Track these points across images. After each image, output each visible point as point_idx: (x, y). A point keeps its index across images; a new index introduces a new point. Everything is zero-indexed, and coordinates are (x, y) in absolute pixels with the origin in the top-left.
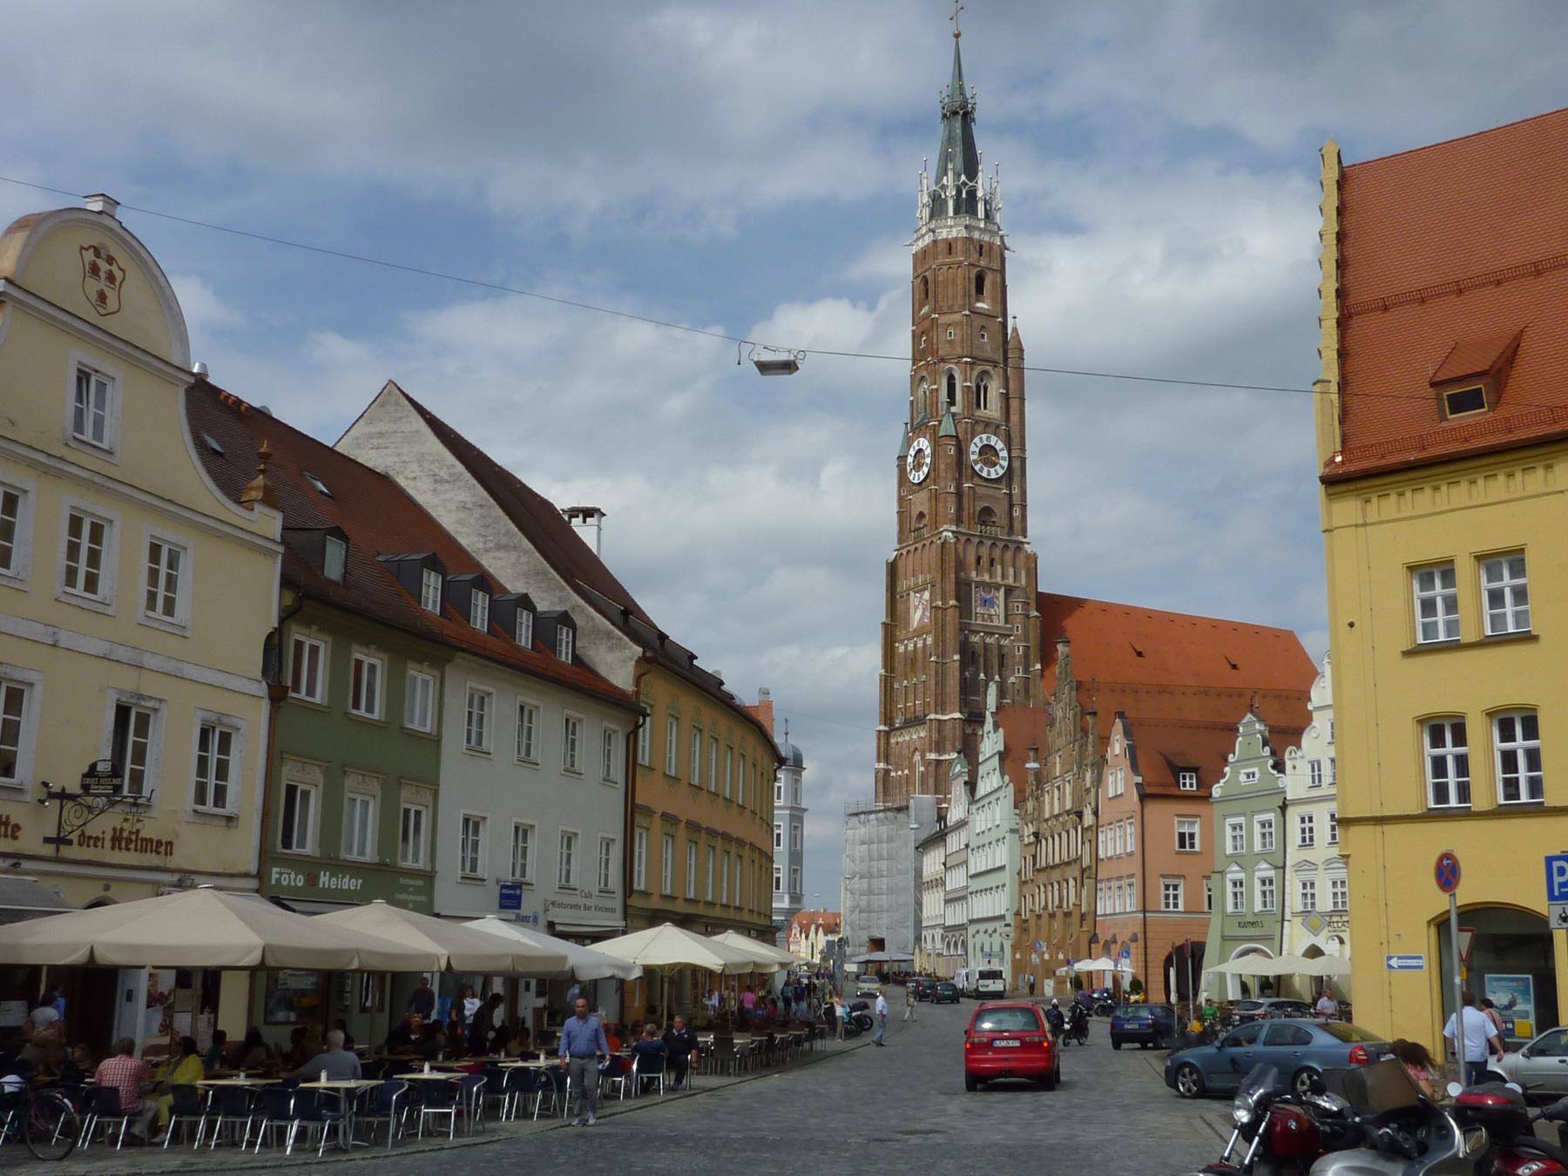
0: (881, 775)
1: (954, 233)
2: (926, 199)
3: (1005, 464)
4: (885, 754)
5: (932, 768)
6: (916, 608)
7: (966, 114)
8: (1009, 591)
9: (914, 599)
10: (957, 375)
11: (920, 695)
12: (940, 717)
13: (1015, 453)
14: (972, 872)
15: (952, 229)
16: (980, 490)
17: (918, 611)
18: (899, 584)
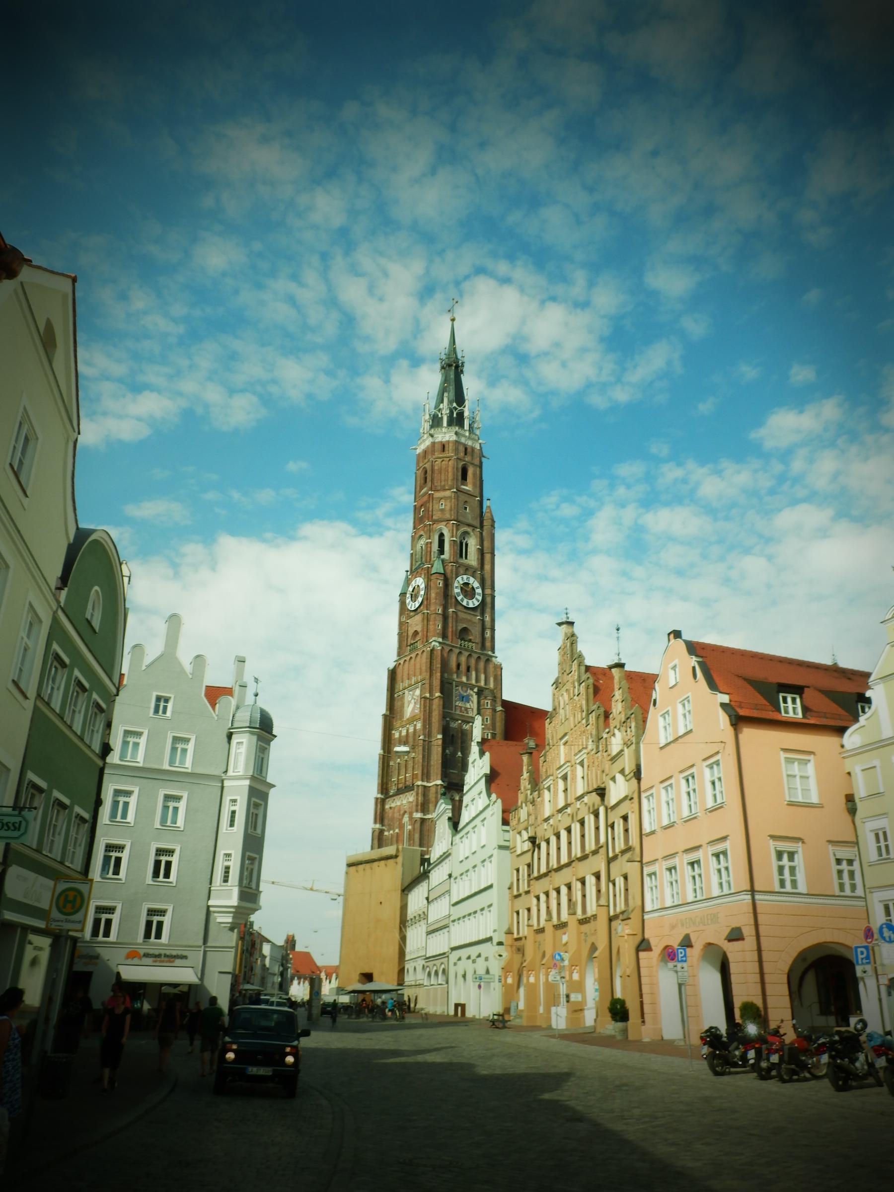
0: (377, 833)
2: (427, 417)
3: (480, 598)
4: (381, 816)
5: (418, 825)
6: (409, 702)
7: (457, 367)
8: (480, 693)
10: (446, 532)
11: (410, 769)
12: (425, 784)
13: (488, 591)
14: (454, 900)
15: (446, 435)
16: (461, 615)
17: (411, 705)
18: (397, 686)
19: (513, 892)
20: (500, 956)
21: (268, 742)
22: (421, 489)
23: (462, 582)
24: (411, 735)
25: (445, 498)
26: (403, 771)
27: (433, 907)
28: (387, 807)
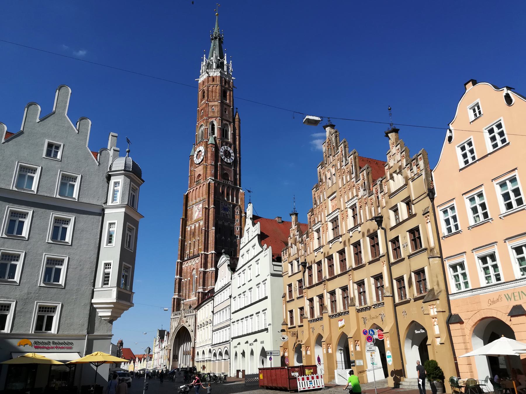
0: (177, 281)
1: (215, 75)
2: (204, 63)
3: (233, 158)
5: (202, 275)
6: (196, 211)
7: (220, 39)
9: (195, 208)
12: (206, 253)
14: (233, 311)
19: (286, 299)
20: (284, 338)
21: (139, 185)
22: (202, 101)
24: (197, 228)
25: (215, 106)
26: (192, 247)
27: (216, 316)
28: (183, 266)
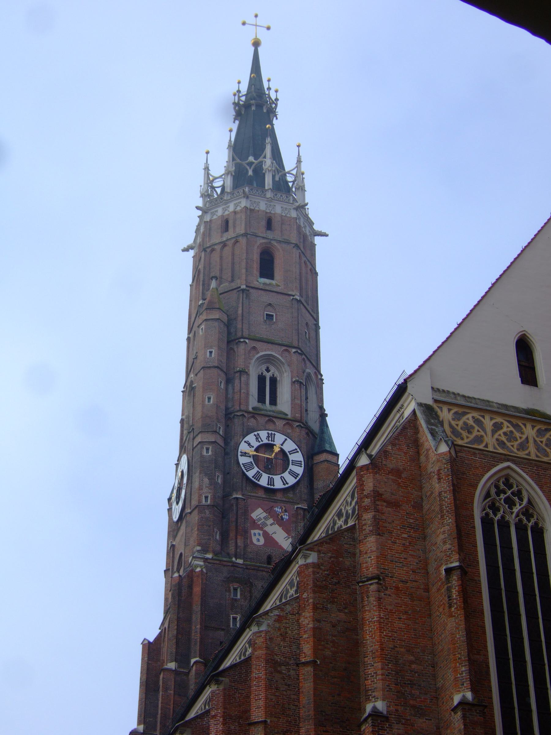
3: (300, 470)
23: (256, 444)
